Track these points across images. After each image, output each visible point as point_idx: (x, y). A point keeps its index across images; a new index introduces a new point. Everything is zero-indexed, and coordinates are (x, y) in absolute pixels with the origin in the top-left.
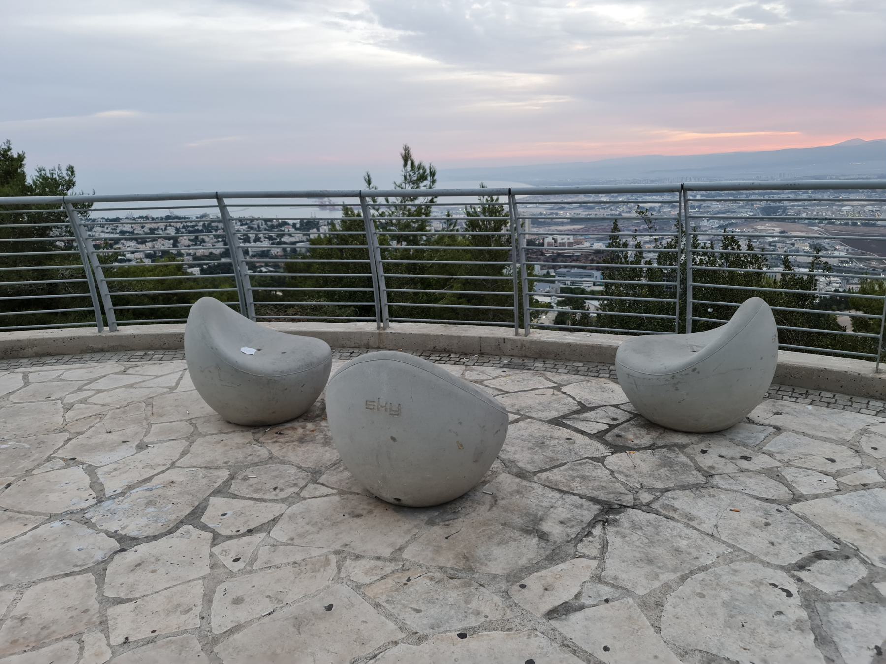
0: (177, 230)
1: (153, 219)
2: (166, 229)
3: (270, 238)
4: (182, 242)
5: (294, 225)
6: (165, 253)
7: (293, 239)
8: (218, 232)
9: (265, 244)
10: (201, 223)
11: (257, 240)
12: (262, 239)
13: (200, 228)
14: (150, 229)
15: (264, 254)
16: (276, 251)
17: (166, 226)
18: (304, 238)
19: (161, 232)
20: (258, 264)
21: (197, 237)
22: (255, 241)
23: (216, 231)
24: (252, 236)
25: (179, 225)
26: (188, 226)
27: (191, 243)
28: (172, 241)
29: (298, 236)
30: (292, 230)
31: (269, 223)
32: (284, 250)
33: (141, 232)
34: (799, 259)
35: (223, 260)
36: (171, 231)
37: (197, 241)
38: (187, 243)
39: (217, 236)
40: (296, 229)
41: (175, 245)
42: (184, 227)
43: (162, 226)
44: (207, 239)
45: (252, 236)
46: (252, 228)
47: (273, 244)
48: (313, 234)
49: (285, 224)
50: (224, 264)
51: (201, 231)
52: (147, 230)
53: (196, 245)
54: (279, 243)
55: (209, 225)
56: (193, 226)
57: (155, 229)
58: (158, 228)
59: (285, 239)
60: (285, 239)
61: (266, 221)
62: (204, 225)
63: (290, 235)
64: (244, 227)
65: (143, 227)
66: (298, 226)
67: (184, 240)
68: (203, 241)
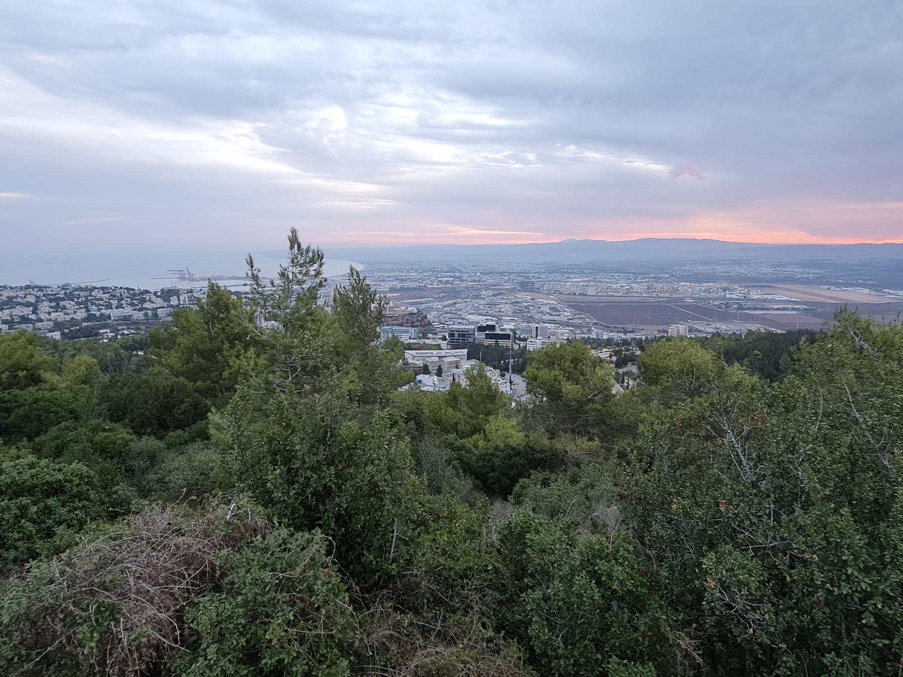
0: (37, 297)
1: (11, 288)
3: (132, 305)
4: (42, 309)
5: (155, 293)
6: (24, 319)
7: (155, 306)
8: (80, 300)
9: (127, 311)
10: (63, 292)
11: (119, 306)
12: (124, 306)
14: (8, 297)
15: (126, 319)
16: (138, 315)
18: (165, 304)
19: (20, 300)
20: (120, 328)
21: (58, 304)
22: (117, 308)
23: (78, 298)
24: (114, 303)
25: (40, 294)
27: (52, 310)
28: (31, 308)
29: (159, 302)
30: (153, 298)
31: (131, 292)
32: (146, 315)
34: (544, 317)
35: (84, 324)
36: (32, 299)
37: (57, 308)
38: (48, 309)
39: (78, 303)
40: (158, 297)
41: (34, 312)
42: (44, 295)
43: (21, 294)
44: (68, 306)
45: (114, 303)
46: (115, 296)
47: (135, 310)
48: (174, 301)
49: (147, 292)
50: (87, 327)
51: (63, 299)
53: (57, 311)
54: (140, 310)
55: (71, 293)
56: (54, 295)
57: (13, 297)
58: (17, 296)
59: (146, 305)
60: (146, 305)
61: (128, 289)
63: (152, 302)
64: (107, 295)
66: (159, 294)
67: (45, 306)
68: (64, 308)
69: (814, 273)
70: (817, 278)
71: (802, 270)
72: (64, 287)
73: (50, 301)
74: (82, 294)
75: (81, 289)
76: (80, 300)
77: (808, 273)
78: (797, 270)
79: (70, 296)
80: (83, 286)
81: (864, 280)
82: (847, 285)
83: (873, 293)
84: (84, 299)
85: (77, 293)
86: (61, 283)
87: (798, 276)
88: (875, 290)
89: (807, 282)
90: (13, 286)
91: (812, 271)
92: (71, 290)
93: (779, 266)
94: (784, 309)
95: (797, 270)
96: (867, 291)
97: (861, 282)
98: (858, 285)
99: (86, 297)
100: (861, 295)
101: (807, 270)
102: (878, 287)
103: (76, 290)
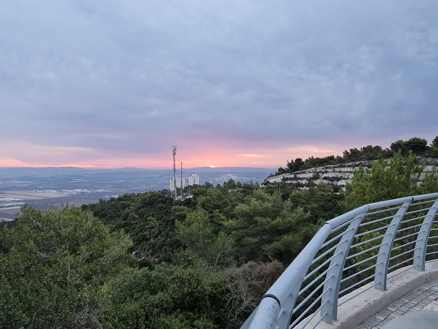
69: (28, 184)
70: (29, 186)
71: (20, 182)
77: (24, 184)
78: (17, 182)
81: (53, 186)
82: (46, 189)
83: (58, 192)
87: (19, 186)
88: (59, 191)
89: (24, 189)
91: (26, 182)
93: (6, 180)
94: (12, 206)
95: (17, 182)
96: (55, 191)
97: (52, 187)
98: (51, 189)
100: (53, 194)
101: (23, 182)
102: (60, 189)
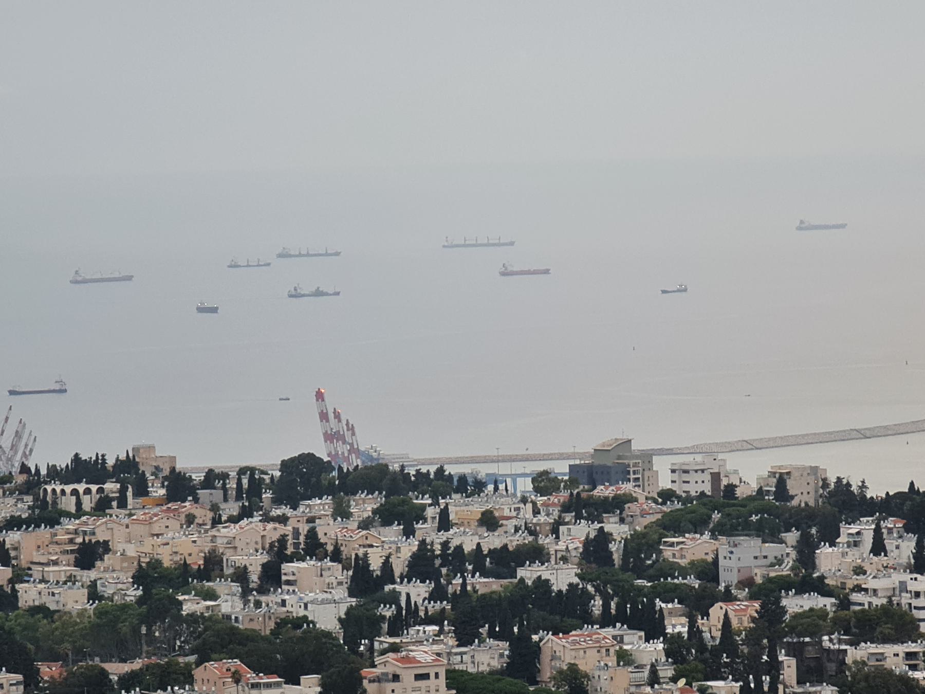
0: (366, 582)
1: (179, 487)
2: (272, 577)
8: (711, 626)
10: (579, 532)
13: (562, 578)
14: (148, 575)
17: (279, 553)
19: (228, 602)
23: (697, 604)
25: (390, 547)
26: (456, 559)
33: (74, 601)
36: (319, 599)
42: (421, 566)
43: (246, 542)
51: (567, 611)
52: (116, 581)
55: (642, 545)
56: (504, 561)
57: (184, 576)
58: (213, 565)
62: (596, 549)
65: (88, 555)
72: (587, 489)
73: (467, 621)
74: (746, 557)
75: (724, 510)
76: (711, 626)
79: (627, 587)
80: (750, 474)
84: (743, 613)
85: (693, 547)
86: (569, 442)
90: (193, 464)
92: (645, 514)
99: (768, 593)
103: (689, 515)
